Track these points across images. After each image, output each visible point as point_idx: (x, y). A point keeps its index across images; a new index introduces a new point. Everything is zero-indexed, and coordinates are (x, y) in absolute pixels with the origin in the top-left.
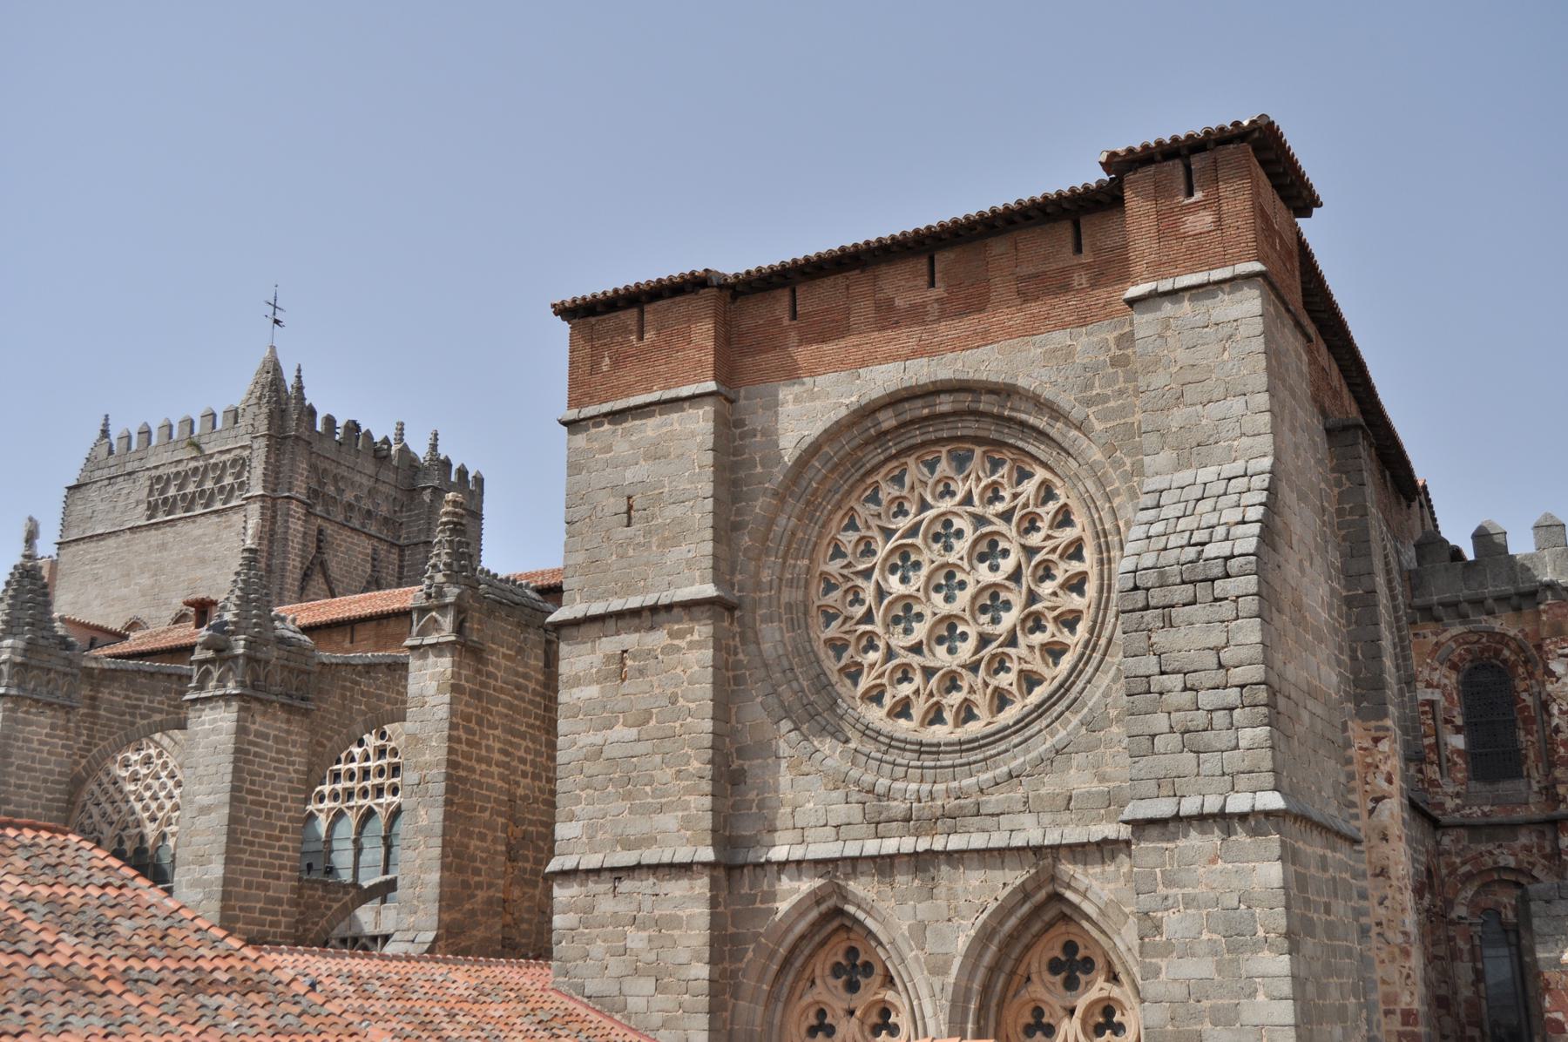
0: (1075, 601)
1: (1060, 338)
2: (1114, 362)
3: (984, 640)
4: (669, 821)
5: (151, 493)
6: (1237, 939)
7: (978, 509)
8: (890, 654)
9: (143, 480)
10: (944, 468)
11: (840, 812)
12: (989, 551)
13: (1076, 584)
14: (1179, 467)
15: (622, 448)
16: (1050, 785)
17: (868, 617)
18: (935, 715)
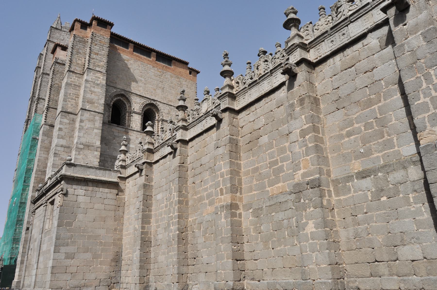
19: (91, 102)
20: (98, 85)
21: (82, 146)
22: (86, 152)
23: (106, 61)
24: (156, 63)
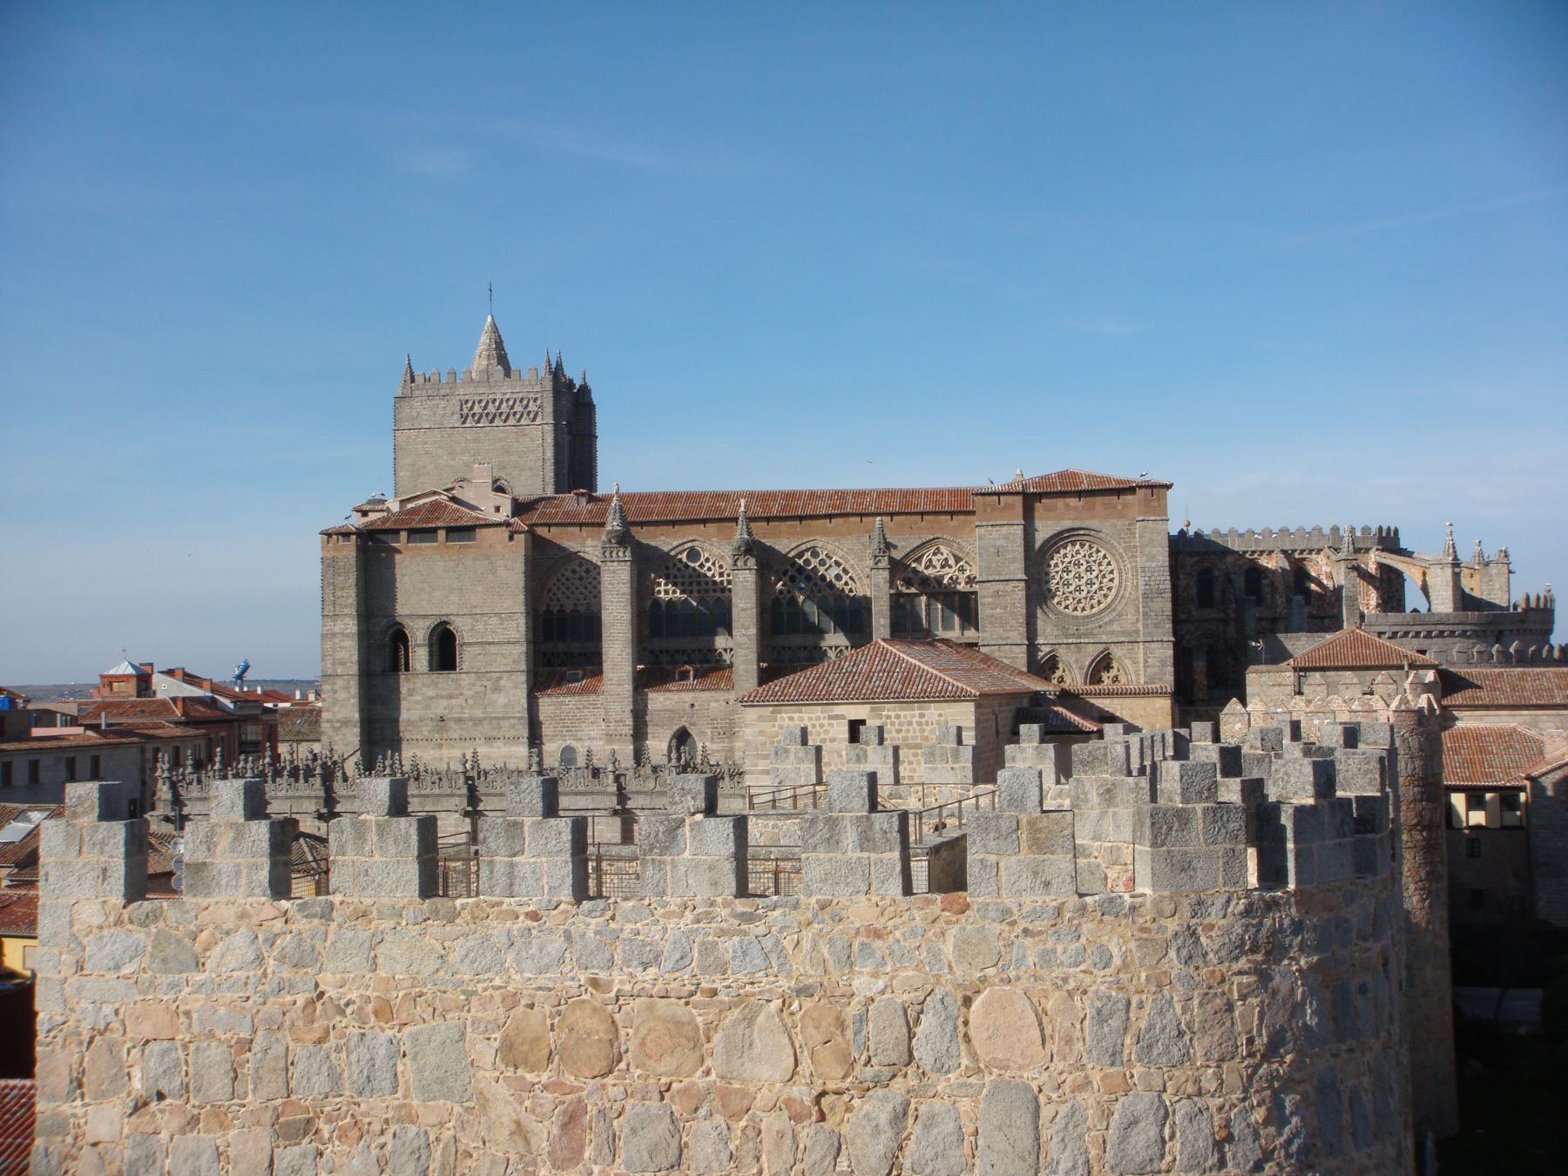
0: (1111, 584)
1: (1114, 521)
2: (1128, 529)
3: (1088, 592)
4: (1014, 634)
5: (462, 410)
6: (1163, 664)
7: (1087, 558)
8: (1064, 593)
9: (455, 402)
10: (1078, 546)
11: (1056, 632)
12: (1089, 570)
13: (1112, 580)
14: (1148, 561)
15: (995, 535)
16: (1109, 628)
17: (1058, 584)
18: (1075, 609)
19: (342, 663)
20: (347, 636)
21: (338, 725)
22: (345, 730)
23: (354, 595)
24: (447, 547)
